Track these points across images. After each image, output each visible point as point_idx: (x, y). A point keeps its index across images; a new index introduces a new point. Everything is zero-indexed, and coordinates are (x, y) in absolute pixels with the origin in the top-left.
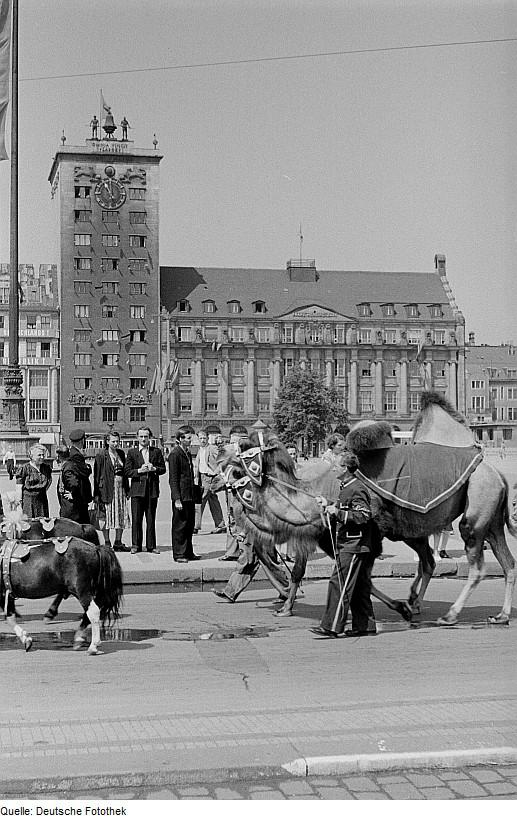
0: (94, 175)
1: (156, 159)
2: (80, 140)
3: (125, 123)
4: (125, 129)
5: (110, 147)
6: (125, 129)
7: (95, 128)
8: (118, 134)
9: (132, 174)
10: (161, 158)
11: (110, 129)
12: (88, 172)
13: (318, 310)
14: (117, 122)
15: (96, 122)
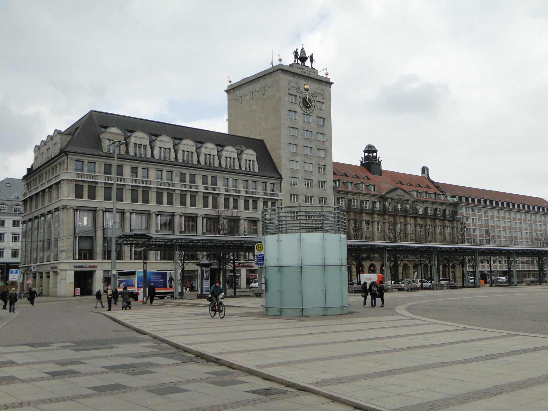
0: (299, 88)
1: (331, 84)
2: (289, 60)
3: (311, 57)
4: (312, 61)
5: (306, 71)
6: (312, 61)
7: (296, 57)
8: (308, 63)
9: (318, 92)
10: (331, 84)
11: (303, 59)
12: (295, 86)
13: (402, 191)
14: (308, 55)
15: (296, 53)
